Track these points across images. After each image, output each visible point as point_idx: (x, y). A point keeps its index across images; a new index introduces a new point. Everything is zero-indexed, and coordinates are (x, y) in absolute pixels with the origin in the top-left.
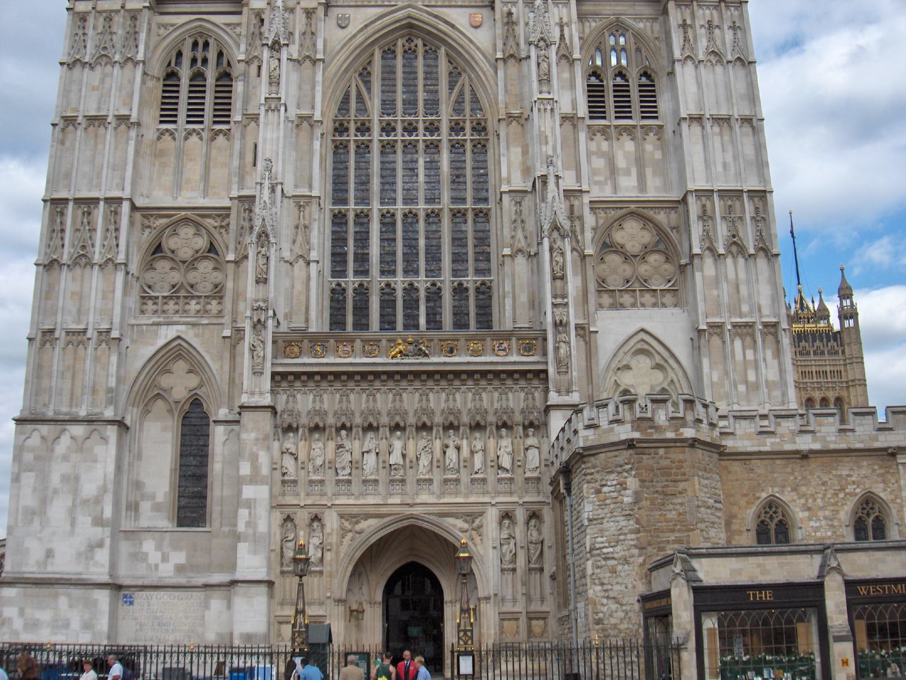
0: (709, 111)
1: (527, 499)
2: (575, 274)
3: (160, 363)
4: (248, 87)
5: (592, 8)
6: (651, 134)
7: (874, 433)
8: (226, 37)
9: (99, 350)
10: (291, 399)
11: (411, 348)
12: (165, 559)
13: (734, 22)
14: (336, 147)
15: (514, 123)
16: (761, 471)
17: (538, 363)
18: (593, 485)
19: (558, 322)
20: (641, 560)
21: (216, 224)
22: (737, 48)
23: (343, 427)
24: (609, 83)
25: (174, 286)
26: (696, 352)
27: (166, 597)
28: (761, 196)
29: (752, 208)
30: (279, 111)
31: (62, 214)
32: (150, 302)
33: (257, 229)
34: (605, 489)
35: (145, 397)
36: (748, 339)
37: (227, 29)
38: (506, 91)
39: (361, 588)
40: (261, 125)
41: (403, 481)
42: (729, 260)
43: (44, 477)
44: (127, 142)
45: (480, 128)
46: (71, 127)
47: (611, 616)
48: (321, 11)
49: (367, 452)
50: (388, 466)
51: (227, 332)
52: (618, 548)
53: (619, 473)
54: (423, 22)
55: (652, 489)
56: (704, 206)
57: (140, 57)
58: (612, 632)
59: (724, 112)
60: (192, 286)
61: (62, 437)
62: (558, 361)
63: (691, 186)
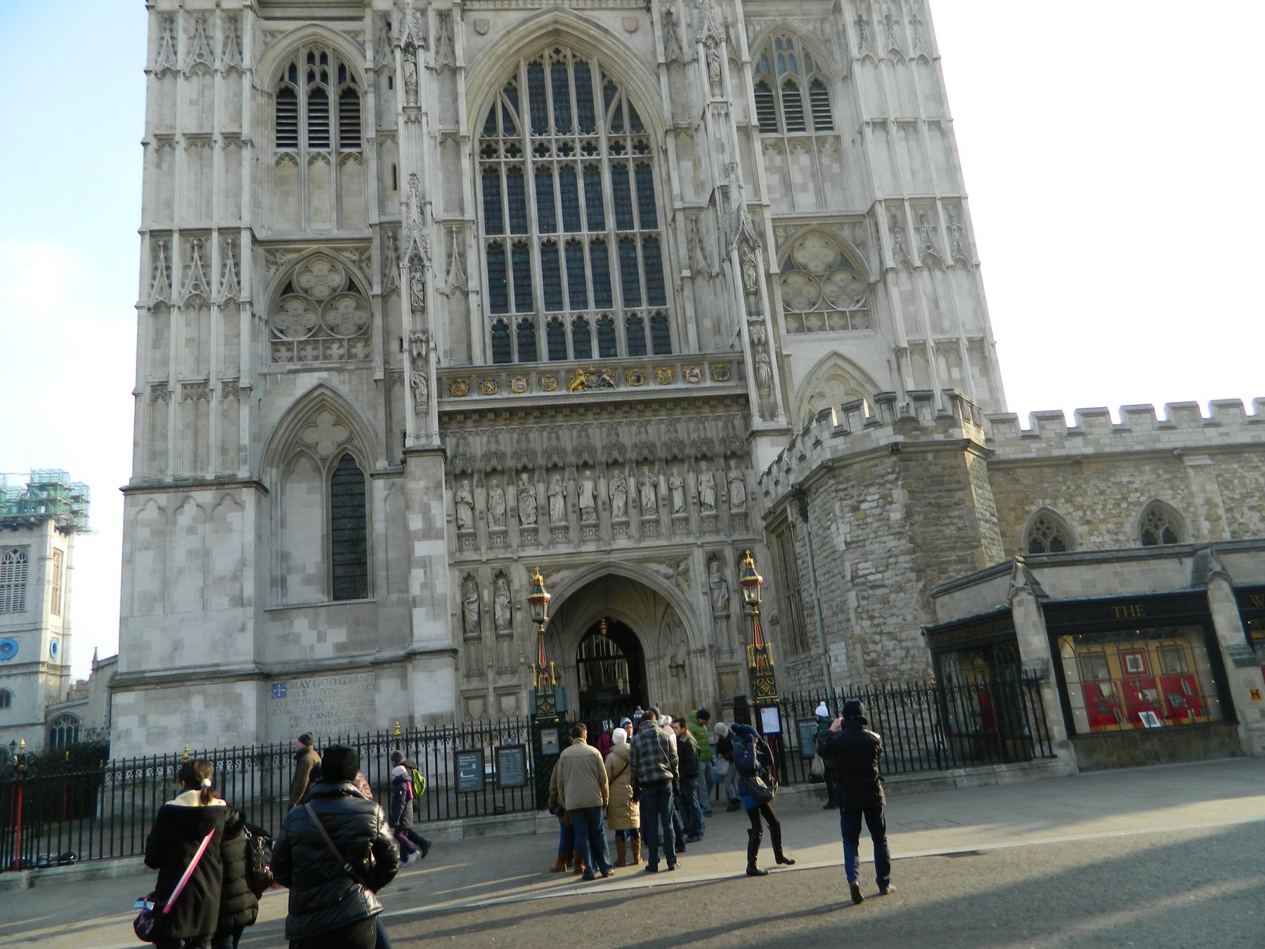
0: (893, 115)
1: (735, 537)
3: (300, 416)
6: (828, 146)
7: (1154, 432)
11: (594, 378)
12: (321, 638)
13: (914, 16)
14: (485, 170)
15: (682, 135)
16: (1028, 481)
18: (849, 502)
19: (756, 340)
20: (921, 585)
23: (525, 469)
24: (778, 93)
25: (310, 330)
26: (895, 373)
27: (325, 682)
28: (956, 204)
30: (420, 122)
31: (167, 248)
32: (283, 349)
34: (863, 506)
36: (952, 357)
37: (348, 37)
38: (672, 100)
39: (553, 652)
41: (596, 526)
42: (926, 274)
43: (164, 555)
44: (240, 164)
45: (641, 147)
46: (167, 148)
47: (888, 655)
48: (457, 14)
52: (888, 574)
53: (882, 485)
54: (573, 28)
55: (924, 501)
56: (894, 217)
57: (247, 63)
58: (891, 675)
59: (908, 115)
60: (332, 330)
61: (186, 506)
62: (759, 385)
63: (880, 195)
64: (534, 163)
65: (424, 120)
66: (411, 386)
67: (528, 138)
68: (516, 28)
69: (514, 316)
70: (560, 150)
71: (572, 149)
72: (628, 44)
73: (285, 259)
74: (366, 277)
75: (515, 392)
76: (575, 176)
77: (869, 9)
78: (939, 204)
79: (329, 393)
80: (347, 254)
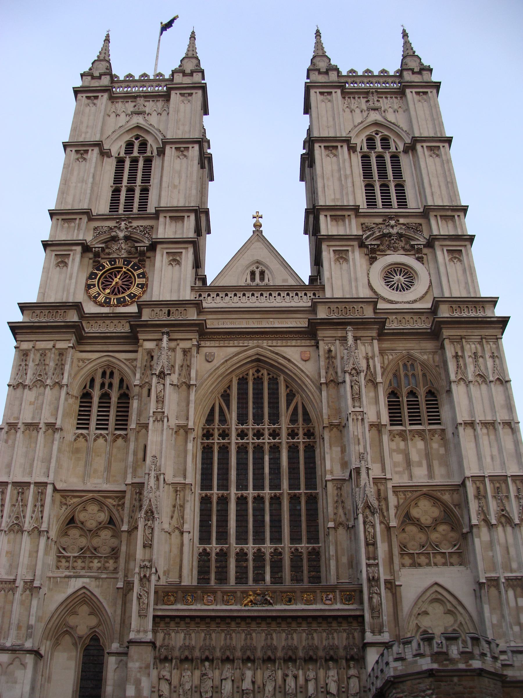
0: (479, 417)
2: (383, 541)
3: (69, 607)
4: (141, 404)
5: (389, 346)
8: (126, 369)
9: (24, 596)
10: (167, 636)
13: (493, 353)
14: (204, 448)
15: (335, 429)
17: (356, 610)
19: (371, 578)
21: (114, 503)
22: (496, 372)
23: (207, 659)
25: (82, 549)
29: (515, 488)
30: (163, 421)
33: (145, 508)
35: (57, 633)
37: (127, 363)
38: (329, 406)
40: (150, 432)
45: (309, 434)
46: (13, 431)
48: (194, 350)
49: (225, 679)
50: (241, 691)
51: (120, 585)
56: (478, 488)
57: (65, 381)
59: (489, 418)
60: (95, 549)
62: (372, 609)
63: (468, 474)
64: (237, 443)
65: (166, 420)
66: (138, 597)
67: (234, 427)
68: (231, 358)
69: (214, 547)
70: (254, 435)
71: (263, 435)
72: (304, 369)
73: (72, 502)
74: (120, 516)
75: (205, 605)
76: (263, 452)
77: (462, 348)
78: (509, 480)
79: (89, 594)
80: (110, 500)
